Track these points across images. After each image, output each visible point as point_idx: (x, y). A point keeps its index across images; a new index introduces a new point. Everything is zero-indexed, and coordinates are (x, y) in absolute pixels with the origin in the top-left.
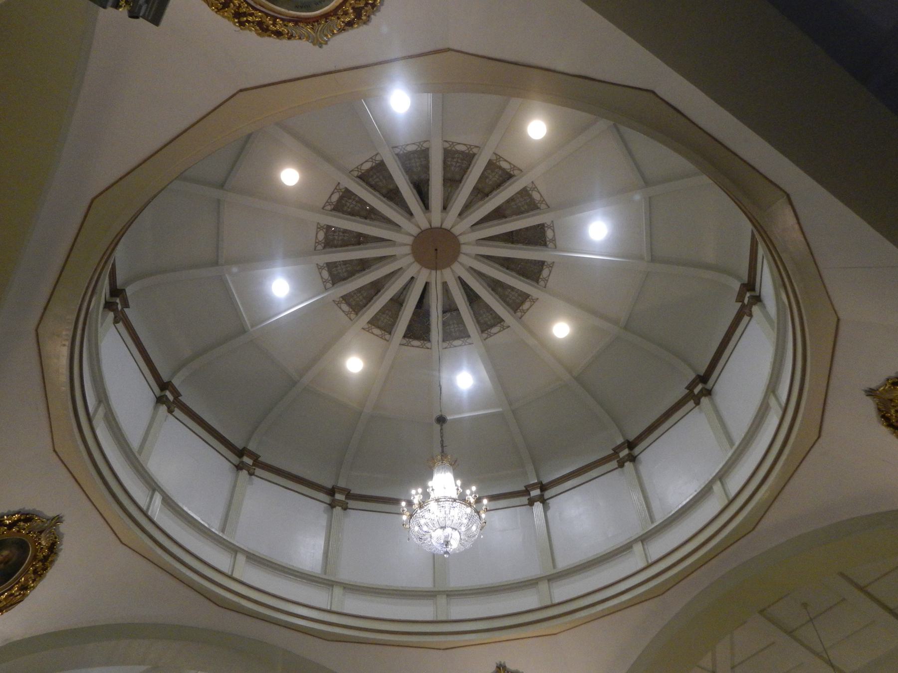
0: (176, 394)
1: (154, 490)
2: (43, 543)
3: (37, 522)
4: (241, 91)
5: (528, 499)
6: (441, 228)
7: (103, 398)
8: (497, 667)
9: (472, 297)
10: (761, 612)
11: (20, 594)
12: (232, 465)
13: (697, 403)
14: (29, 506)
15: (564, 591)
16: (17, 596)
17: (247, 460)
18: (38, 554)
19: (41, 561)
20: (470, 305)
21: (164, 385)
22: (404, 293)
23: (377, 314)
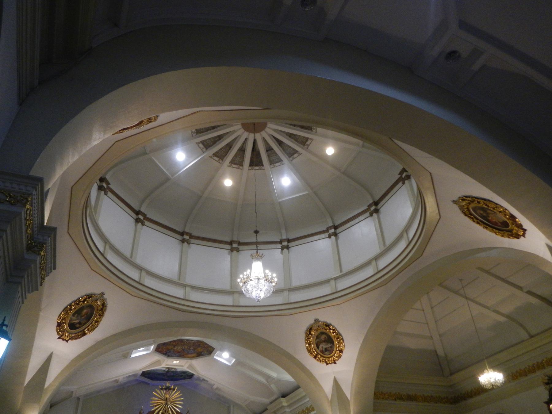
0: (144, 215)
1: (141, 270)
2: (99, 304)
3: (94, 297)
4: (117, 141)
5: (328, 235)
7: (106, 241)
8: (315, 320)
9: (280, 143)
10: (440, 285)
12: (179, 241)
13: (404, 183)
14: (89, 292)
15: (343, 284)
17: (186, 237)
18: (98, 308)
19: (100, 310)
20: (280, 145)
21: (138, 213)
22: (244, 146)
23: (233, 158)
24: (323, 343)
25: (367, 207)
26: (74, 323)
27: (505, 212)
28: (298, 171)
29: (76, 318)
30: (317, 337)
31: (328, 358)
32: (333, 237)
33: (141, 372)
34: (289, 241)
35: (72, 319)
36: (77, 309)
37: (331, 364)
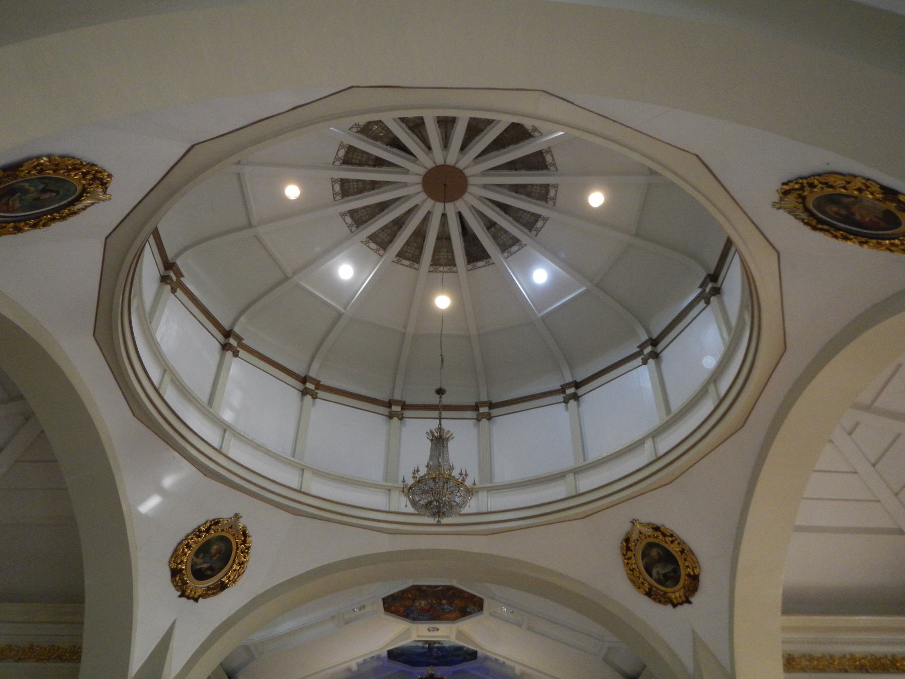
6: (437, 166)
9: (504, 208)
11: (240, 568)
16: (239, 570)
20: (506, 213)
24: (658, 565)
25: (701, 290)
26: (201, 568)
27: (867, 187)
28: (552, 253)
29: (202, 561)
30: (644, 556)
31: (674, 592)
32: (651, 362)
33: (384, 654)
34: (577, 385)
35: (195, 563)
36: (199, 545)
37: (681, 604)
